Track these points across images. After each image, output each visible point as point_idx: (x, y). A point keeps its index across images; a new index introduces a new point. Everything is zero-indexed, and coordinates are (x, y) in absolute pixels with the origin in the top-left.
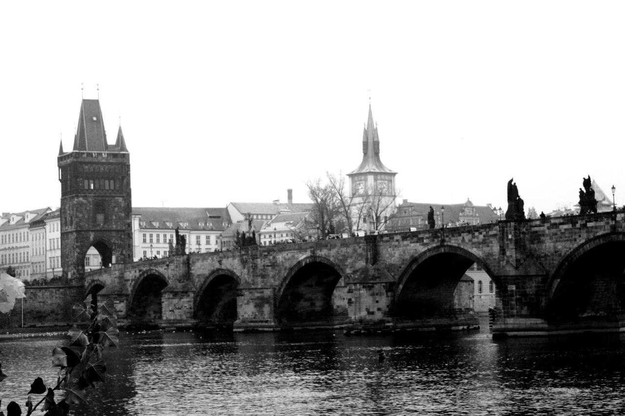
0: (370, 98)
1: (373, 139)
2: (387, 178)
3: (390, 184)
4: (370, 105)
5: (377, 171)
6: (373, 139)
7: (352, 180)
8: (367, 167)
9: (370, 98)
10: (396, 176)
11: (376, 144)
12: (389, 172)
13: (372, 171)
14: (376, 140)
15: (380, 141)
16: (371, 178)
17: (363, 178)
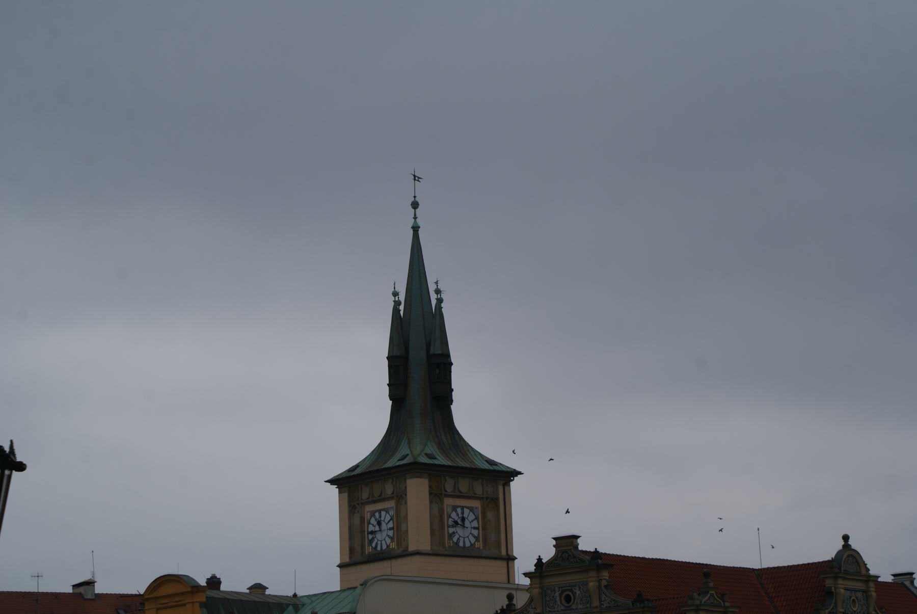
0: (415, 205)
1: (428, 345)
2: (478, 489)
3: (490, 515)
4: (416, 229)
5: (442, 460)
6: (428, 345)
7: (351, 500)
8: (404, 450)
9: (415, 205)
10: (516, 485)
11: (440, 367)
12: (487, 466)
13: (424, 460)
14: (436, 349)
15: (454, 358)
16: (417, 489)
17: (389, 489)
